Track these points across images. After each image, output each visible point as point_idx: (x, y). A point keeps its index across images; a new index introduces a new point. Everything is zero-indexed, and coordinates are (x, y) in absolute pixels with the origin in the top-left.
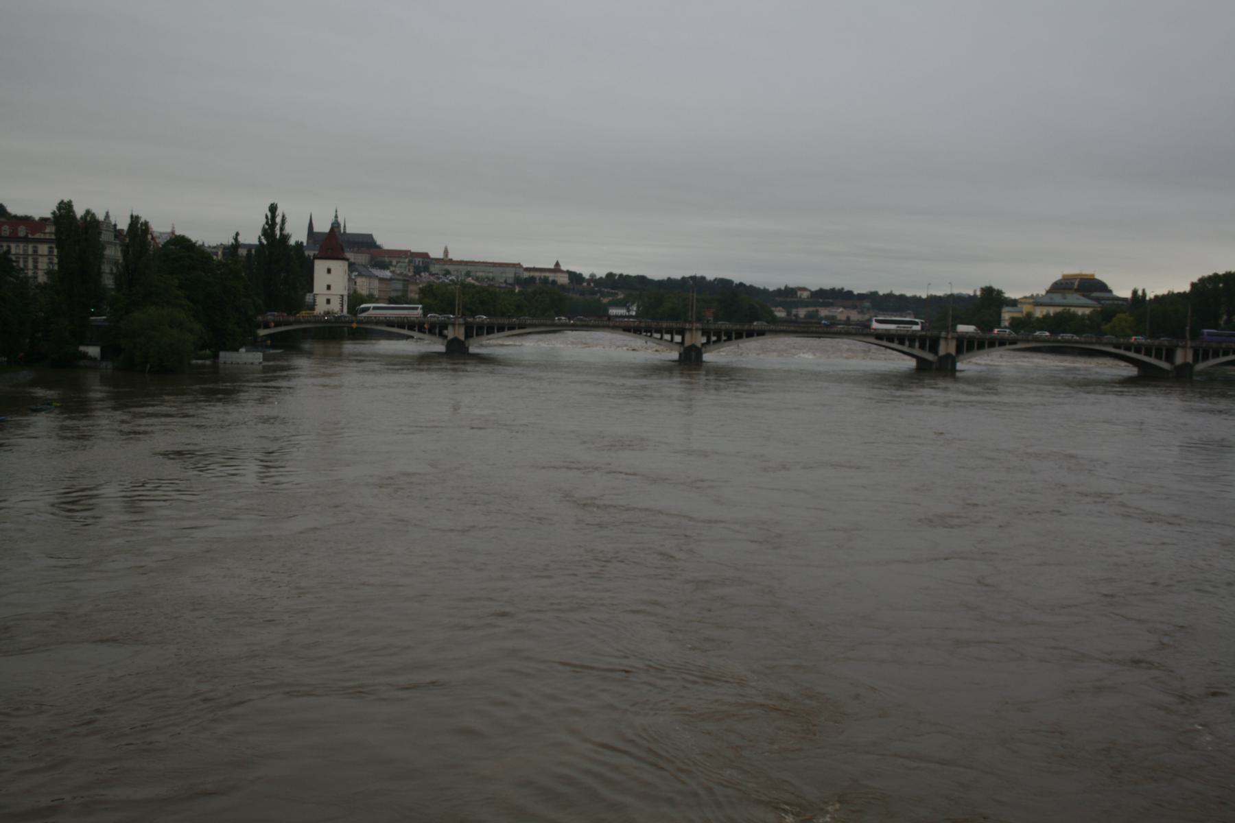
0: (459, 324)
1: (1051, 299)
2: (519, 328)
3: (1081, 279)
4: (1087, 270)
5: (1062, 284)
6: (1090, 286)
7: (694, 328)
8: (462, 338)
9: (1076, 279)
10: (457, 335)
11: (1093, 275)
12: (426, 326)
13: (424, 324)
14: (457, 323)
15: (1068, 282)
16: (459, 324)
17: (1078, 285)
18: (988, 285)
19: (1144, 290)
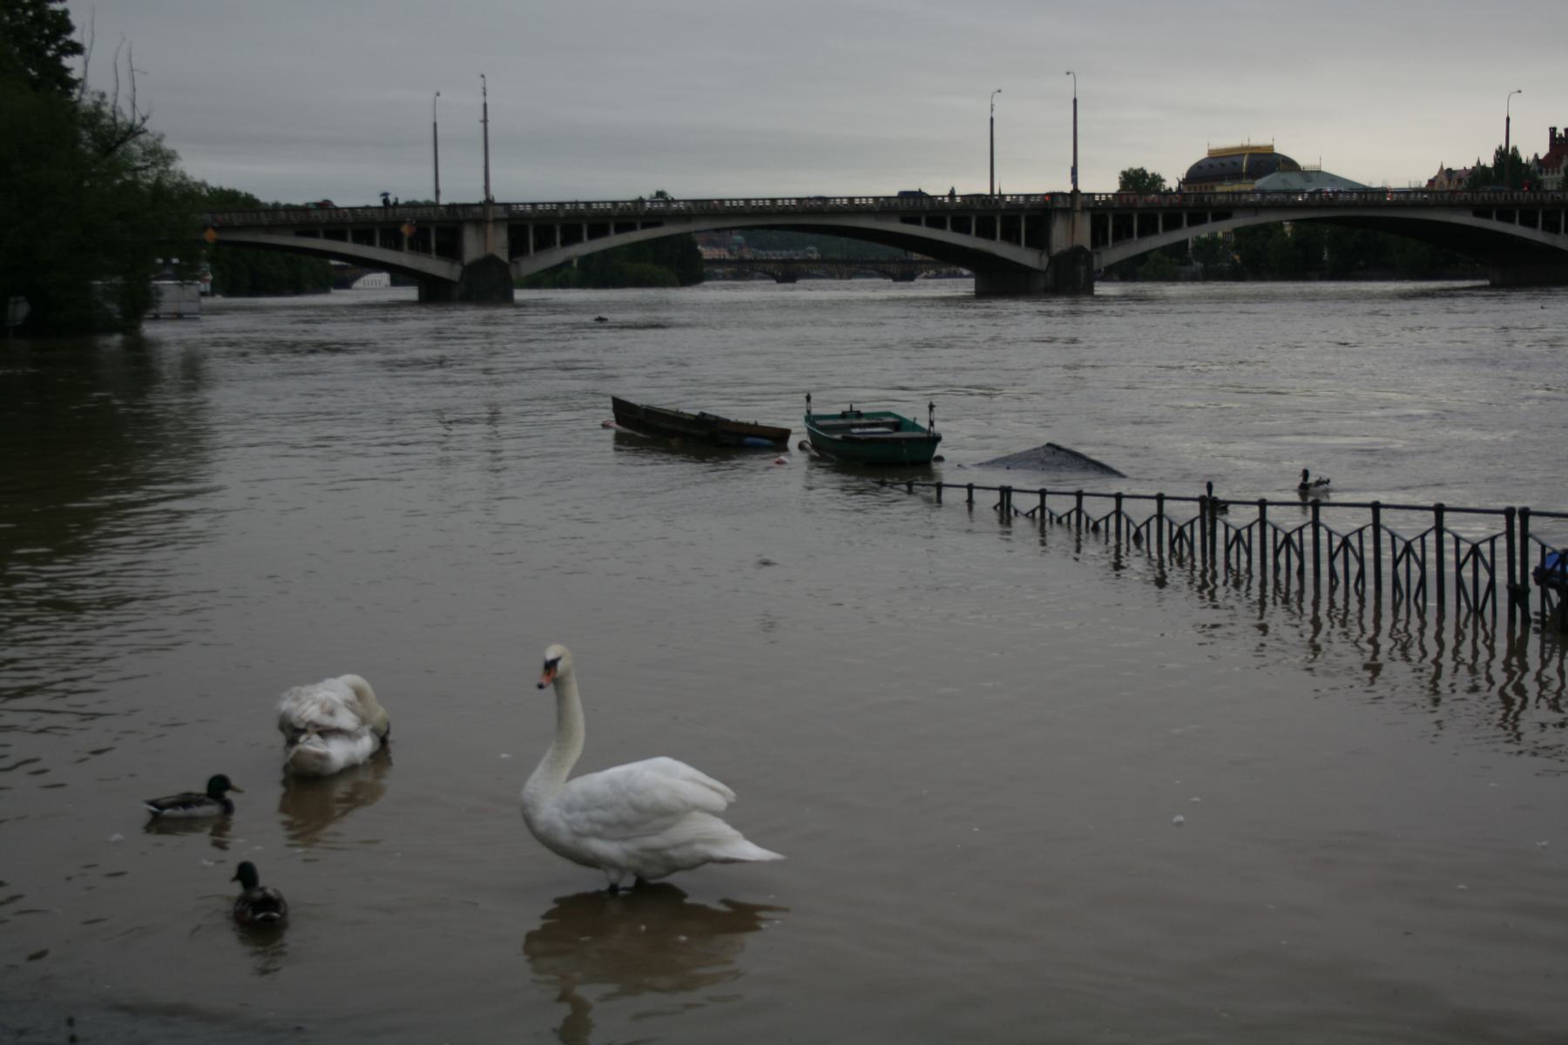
0: (497, 221)
1: (1285, 181)
2: (645, 226)
3: (1251, 155)
4: (1258, 139)
5: (1211, 166)
6: (1266, 161)
7: (1078, 207)
8: (503, 256)
9: (1243, 155)
10: (490, 250)
11: (1271, 147)
12: (405, 230)
13: (402, 222)
14: (491, 217)
15: (1224, 161)
16: (497, 221)
17: (1248, 167)
18: (1136, 166)
19: (1515, 149)
